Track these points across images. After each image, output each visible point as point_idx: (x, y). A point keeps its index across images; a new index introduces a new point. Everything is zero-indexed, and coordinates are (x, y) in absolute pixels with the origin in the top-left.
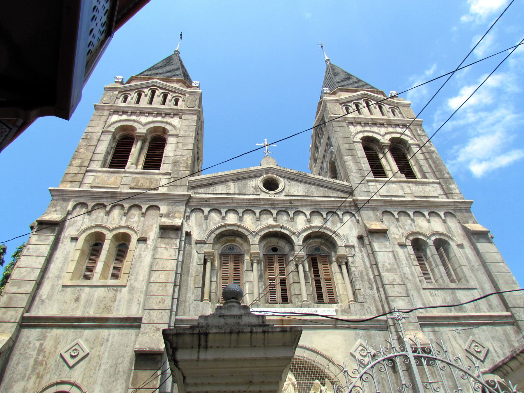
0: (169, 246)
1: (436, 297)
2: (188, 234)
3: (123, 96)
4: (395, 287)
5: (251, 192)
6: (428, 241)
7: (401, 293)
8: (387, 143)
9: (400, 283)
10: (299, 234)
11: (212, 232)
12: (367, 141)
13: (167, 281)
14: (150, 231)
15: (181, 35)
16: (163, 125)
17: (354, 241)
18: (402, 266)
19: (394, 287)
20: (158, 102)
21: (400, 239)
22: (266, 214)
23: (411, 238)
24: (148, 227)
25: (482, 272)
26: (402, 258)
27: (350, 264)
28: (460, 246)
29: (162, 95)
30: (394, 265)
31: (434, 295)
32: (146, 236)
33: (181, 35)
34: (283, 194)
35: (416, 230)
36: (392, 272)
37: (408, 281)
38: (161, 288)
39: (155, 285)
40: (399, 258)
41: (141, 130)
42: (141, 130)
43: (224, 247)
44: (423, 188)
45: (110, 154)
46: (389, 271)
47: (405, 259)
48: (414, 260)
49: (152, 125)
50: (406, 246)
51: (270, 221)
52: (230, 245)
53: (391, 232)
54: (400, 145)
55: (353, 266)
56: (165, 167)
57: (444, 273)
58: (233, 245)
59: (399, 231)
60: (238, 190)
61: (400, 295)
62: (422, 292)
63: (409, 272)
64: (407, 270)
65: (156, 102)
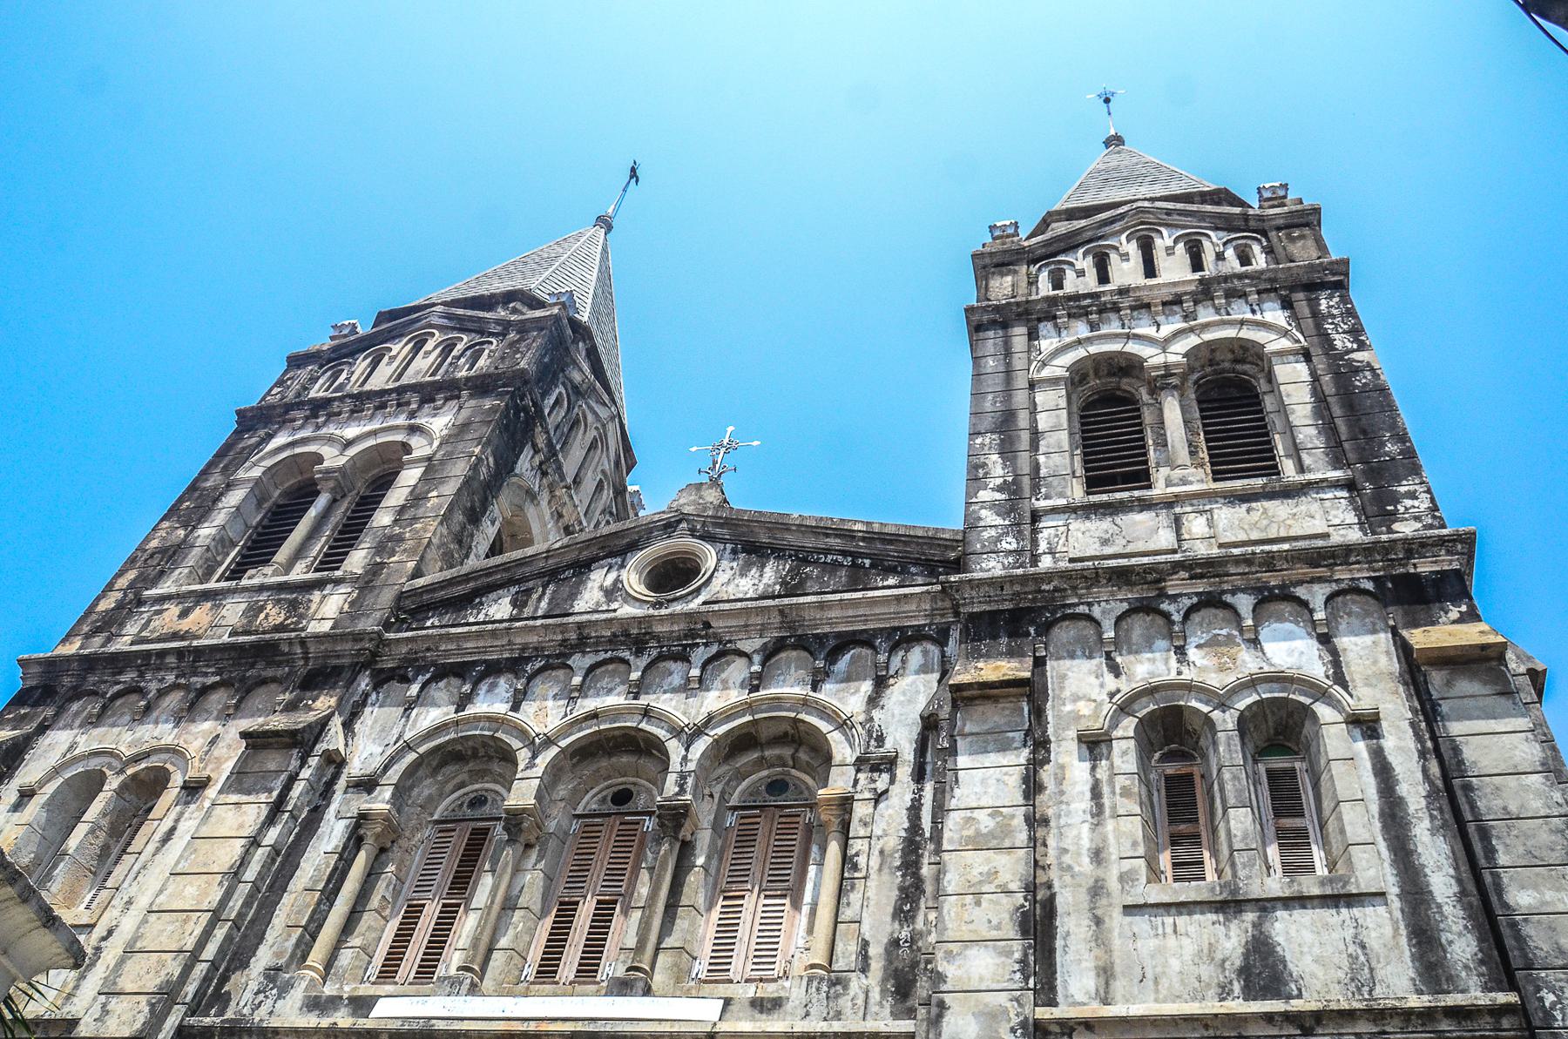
0: (251, 798)
1: (1172, 941)
2: (335, 762)
3: (329, 373)
4: (984, 904)
5: (591, 605)
6: (1216, 715)
7: (998, 927)
8: (1177, 365)
9: (1014, 886)
10: (699, 731)
11: (409, 747)
12: (1111, 374)
13: (198, 903)
14: (227, 760)
15: (633, 170)
16: (399, 437)
17: (901, 738)
18: (1062, 822)
19: (978, 903)
20: (418, 372)
21: (1096, 715)
22: (613, 674)
23: (1147, 708)
24: (229, 746)
25: (1438, 823)
26: (1078, 788)
27: (856, 829)
28: (1366, 725)
29: (440, 348)
30: (1013, 816)
31: (1169, 930)
32: (205, 774)
33: (633, 170)
34: (701, 599)
35: (1179, 673)
36: (994, 843)
37: (1067, 879)
38: (170, 928)
39: (159, 919)
40: (1062, 793)
41: (333, 458)
42: (333, 458)
43: (458, 798)
44: (1265, 511)
45: (234, 545)
46: (979, 843)
47: (1088, 795)
48: (1126, 792)
49: (371, 442)
50: (1111, 740)
51: (616, 699)
52: (476, 791)
53: (1067, 694)
54: (1247, 367)
55: (862, 833)
56: (357, 561)
57: (1245, 837)
58: (487, 790)
59: (1102, 686)
60: (551, 600)
61: (994, 934)
62: (1117, 921)
63: (1086, 843)
64: (1078, 837)
65: (412, 372)
